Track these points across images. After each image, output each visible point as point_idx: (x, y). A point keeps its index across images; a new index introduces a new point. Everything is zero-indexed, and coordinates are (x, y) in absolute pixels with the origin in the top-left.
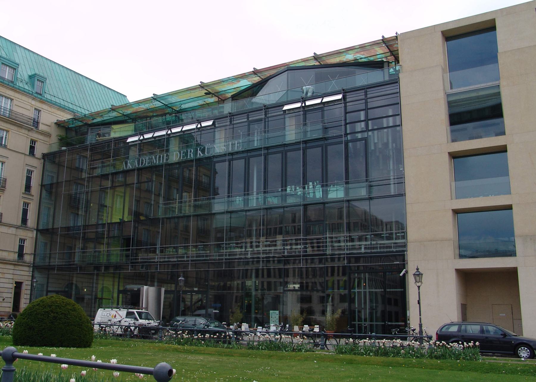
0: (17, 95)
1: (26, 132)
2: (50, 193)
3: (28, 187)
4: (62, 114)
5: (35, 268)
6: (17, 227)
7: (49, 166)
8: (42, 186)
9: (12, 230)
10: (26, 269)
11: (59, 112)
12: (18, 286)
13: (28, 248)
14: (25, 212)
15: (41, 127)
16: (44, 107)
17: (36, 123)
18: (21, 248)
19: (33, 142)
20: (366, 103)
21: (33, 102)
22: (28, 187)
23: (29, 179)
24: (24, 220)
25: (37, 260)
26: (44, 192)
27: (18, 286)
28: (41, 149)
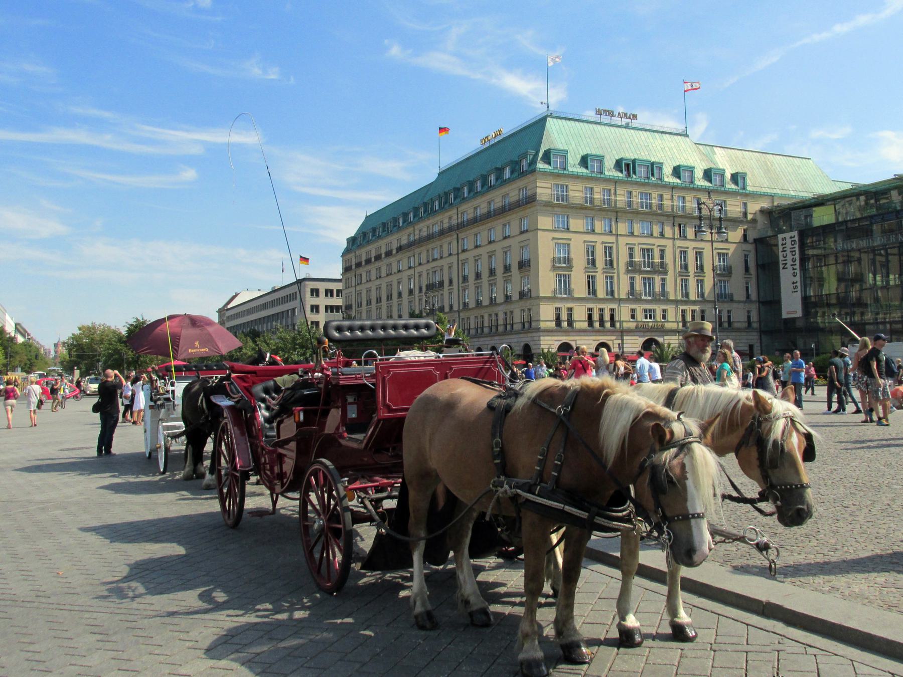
5: (762, 332)
8: (758, 266)
9: (741, 305)
13: (754, 317)
15: (750, 217)
22: (747, 269)
23: (746, 261)
24: (748, 296)
26: (760, 270)
28: (751, 236)
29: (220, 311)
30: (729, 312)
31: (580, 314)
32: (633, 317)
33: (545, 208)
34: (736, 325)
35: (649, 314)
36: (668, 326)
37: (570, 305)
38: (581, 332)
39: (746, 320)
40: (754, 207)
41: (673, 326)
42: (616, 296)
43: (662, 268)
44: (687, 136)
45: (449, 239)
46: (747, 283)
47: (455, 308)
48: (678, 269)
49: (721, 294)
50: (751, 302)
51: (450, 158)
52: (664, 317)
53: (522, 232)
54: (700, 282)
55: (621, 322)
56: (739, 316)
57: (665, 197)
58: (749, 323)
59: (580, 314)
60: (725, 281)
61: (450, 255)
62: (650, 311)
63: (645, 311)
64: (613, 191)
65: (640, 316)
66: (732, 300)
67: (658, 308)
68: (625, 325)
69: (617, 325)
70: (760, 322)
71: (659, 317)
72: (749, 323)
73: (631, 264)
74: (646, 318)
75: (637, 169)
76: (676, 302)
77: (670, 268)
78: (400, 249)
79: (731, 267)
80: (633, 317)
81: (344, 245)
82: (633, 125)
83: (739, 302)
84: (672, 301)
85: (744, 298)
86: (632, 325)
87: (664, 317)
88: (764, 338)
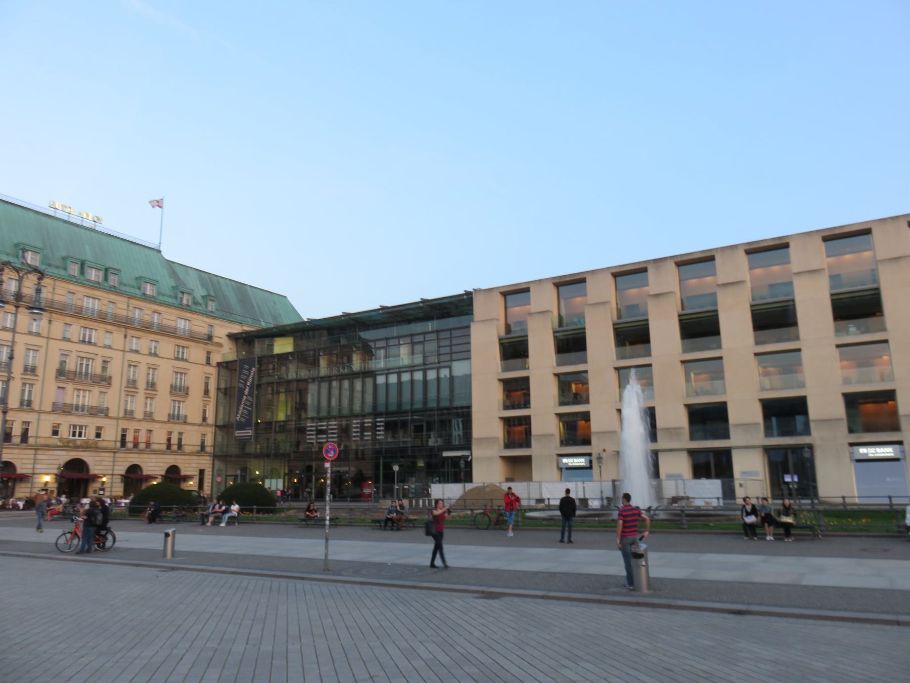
1: (203, 346)
2: (225, 394)
3: (206, 392)
4: (232, 325)
5: (215, 456)
6: (200, 425)
7: (223, 372)
8: (218, 389)
10: (208, 458)
12: (202, 472)
13: (209, 441)
14: (205, 411)
15: (216, 340)
16: (217, 322)
17: (210, 338)
18: (203, 443)
19: (209, 353)
21: (207, 320)
22: (206, 392)
23: (207, 384)
24: (204, 419)
25: (217, 450)
26: (221, 395)
27: (202, 472)
28: (216, 358)
30: (181, 434)
32: (55, 433)
34: (187, 449)
35: (77, 431)
36: (101, 444)
39: (199, 443)
40: (222, 331)
41: (112, 445)
42: (37, 408)
43: (104, 380)
44: (159, 252)
46: (205, 405)
48: (124, 383)
49: (174, 414)
50: (208, 425)
52: (98, 435)
55: (37, 437)
56: (192, 438)
57: (119, 305)
60: (179, 402)
62: (81, 427)
63: (75, 426)
64: (51, 290)
66: (185, 423)
67: (91, 424)
68: (41, 441)
69: (31, 441)
70: (214, 446)
71: (92, 436)
73: (61, 373)
74: (74, 435)
75: (87, 270)
76: (118, 419)
77: (116, 382)
79: (188, 388)
80: (55, 433)
82: (98, 229)
85: (199, 421)
86: (55, 441)
87: (98, 435)
88: (218, 464)
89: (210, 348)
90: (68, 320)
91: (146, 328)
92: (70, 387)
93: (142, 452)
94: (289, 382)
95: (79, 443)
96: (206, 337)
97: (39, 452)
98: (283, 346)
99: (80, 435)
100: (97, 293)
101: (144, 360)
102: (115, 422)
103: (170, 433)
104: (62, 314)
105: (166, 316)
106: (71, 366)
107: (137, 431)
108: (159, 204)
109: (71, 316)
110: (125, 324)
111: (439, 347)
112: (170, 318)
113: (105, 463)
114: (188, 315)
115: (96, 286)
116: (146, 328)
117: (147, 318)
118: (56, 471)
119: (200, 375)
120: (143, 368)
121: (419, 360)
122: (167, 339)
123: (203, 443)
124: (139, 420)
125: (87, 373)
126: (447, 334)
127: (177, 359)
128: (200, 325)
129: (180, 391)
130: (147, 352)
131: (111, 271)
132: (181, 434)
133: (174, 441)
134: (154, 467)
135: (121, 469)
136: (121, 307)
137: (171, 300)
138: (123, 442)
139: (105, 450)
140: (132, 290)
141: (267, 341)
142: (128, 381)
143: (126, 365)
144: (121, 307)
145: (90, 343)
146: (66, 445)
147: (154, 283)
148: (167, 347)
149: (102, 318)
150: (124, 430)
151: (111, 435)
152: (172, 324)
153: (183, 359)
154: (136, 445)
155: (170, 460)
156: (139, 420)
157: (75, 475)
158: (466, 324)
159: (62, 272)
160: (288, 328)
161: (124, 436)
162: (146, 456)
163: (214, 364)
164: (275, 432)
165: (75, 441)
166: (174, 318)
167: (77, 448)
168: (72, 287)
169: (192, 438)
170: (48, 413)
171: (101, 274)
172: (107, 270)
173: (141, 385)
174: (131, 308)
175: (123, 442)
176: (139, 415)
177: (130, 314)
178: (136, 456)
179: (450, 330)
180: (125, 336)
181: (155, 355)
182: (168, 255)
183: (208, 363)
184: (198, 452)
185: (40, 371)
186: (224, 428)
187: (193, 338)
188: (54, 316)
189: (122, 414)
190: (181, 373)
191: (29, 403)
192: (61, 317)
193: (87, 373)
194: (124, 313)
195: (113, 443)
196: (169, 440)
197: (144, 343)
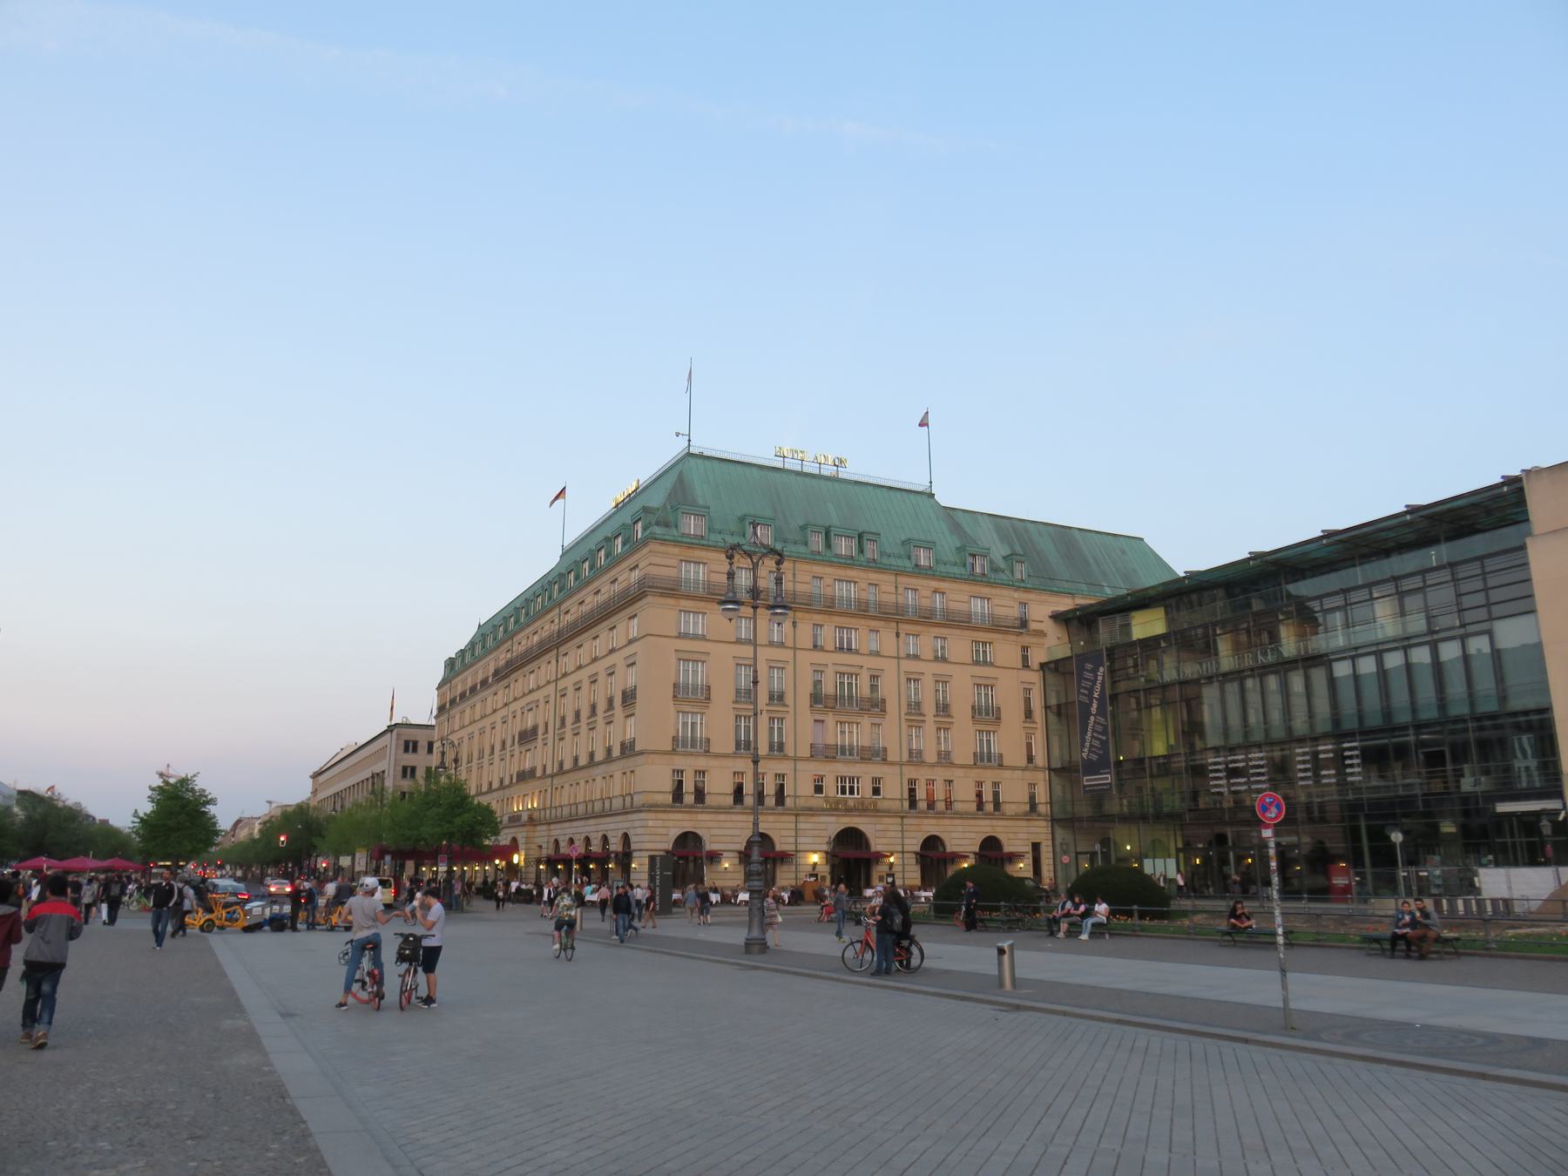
0: (994, 591)
1: (1014, 638)
2: (1059, 714)
3: (1029, 714)
5: (1054, 821)
6: (1025, 769)
7: (1051, 678)
8: (1047, 707)
10: (1043, 823)
11: (1051, 599)
12: (1036, 847)
13: (1042, 795)
14: (1029, 746)
15: (1033, 626)
16: (1032, 596)
17: (1024, 623)
18: (1032, 797)
19: (1025, 649)
20: (1484, 580)
21: (1016, 595)
22: (1029, 714)
23: (1028, 701)
24: (1030, 759)
25: (1056, 808)
26: (1053, 718)
27: (1036, 847)
28: (1038, 656)
29: (315, 776)
30: (996, 784)
31: (719, 785)
32: (819, 789)
33: (662, 600)
34: (1009, 809)
35: (847, 785)
36: (881, 805)
37: (701, 763)
38: (719, 810)
39: (1027, 799)
40: (1041, 609)
41: (896, 805)
42: (791, 754)
43: (876, 706)
45: (547, 657)
47: (549, 771)
50: (1037, 769)
51: (576, 529)
52: (876, 791)
53: (631, 642)
54: (942, 728)
55: (795, 796)
56: (1014, 791)
57: (884, 588)
58: (1033, 805)
59: (719, 785)
60: (988, 732)
61: (549, 682)
62: (852, 779)
63: (843, 779)
65: (830, 788)
66: (1001, 766)
67: (865, 773)
68: (802, 803)
69: (789, 802)
71: (866, 789)
72: (1033, 805)
73: (816, 698)
74: (843, 792)
75: (834, 541)
76: (901, 764)
77: (892, 706)
78: (496, 673)
80: (819, 789)
81: (439, 674)
83: (1014, 768)
84: (892, 764)
85: (1024, 762)
86: (818, 800)
87: (876, 791)
88: (1060, 833)
89: (1026, 640)
90: (818, 618)
91: (926, 618)
92: (830, 719)
93: (940, 815)
94: (1165, 687)
95: (851, 803)
96: (1017, 623)
97: (801, 819)
98: (1148, 625)
99: (852, 792)
100: (852, 573)
101: (930, 670)
102: (897, 768)
103: (980, 784)
104: (808, 611)
105: (952, 596)
106: (828, 688)
107: (930, 782)
108: (923, 423)
109: (819, 612)
110: (894, 616)
111: (1459, 595)
112: (959, 598)
113: (890, 834)
114: (986, 591)
115: (849, 562)
116: (926, 618)
117: (925, 603)
118: (825, 847)
119: (1015, 685)
120: (928, 682)
121: (1417, 624)
122: (958, 632)
123: (1032, 797)
124: (932, 766)
125: (850, 697)
126: (1474, 569)
127: (976, 663)
128: (1006, 604)
129: (987, 715)
130: (931, 657)
131: (866, 537)
132: (996, 784)
133: (988, 796)
134: (963, 839)
135: (915, 844)
136: (886, 590)
137: (956, 570)
138: (913, 802)
139: (889, 813)
140: (900, 562)
141: (1118, 620)
142: (909, 705)
143: (903, 680)
144: (886, 590)
145: (849, 649)
146: (835, 808)
147: (929, 546)
148: (959, 646)
149: (862, 611)
150: (912, 782)
151: (894, 790)
152: (963, 607)
153: (985, 663)
154: (931, 805)
155: (985, 828)
156: (932, 766)
157: (852, 853)
158: (1515, 543)
159: (802, 549)
160: (1152, 593)
161: (912, 791)
162: (948, 822)
163: (1036, 666)
164: (1152, 776)
165: (846, 801)
166: (966, 598)
167: (849, 811)
168: (818, 569)
169: (1014, 791)
170: (807, 759)
171: (854, 543)
172: (860, 536)
173: (929, 709)
174: (900, 590)
175: (913, 802)
176: (931, 757)
177: (901, 600)
178: (933, 821)
179: (1481, 559)
180: (898, 635)
181: (944, 660)
182: (945, 498)
183: (1026, 666)
184: (1026, 814)
185: (789, 699)
186: (1064, 772)
187: (997, 626)
188: (799, 614)
189: (905, 757)
190: (986, 686)
191: (781, 746)
192: (807, 616)
193: (850, 697)
194: (891, 599)
195: (898, 803)
196: (979, 795)
197: (924, 642)
